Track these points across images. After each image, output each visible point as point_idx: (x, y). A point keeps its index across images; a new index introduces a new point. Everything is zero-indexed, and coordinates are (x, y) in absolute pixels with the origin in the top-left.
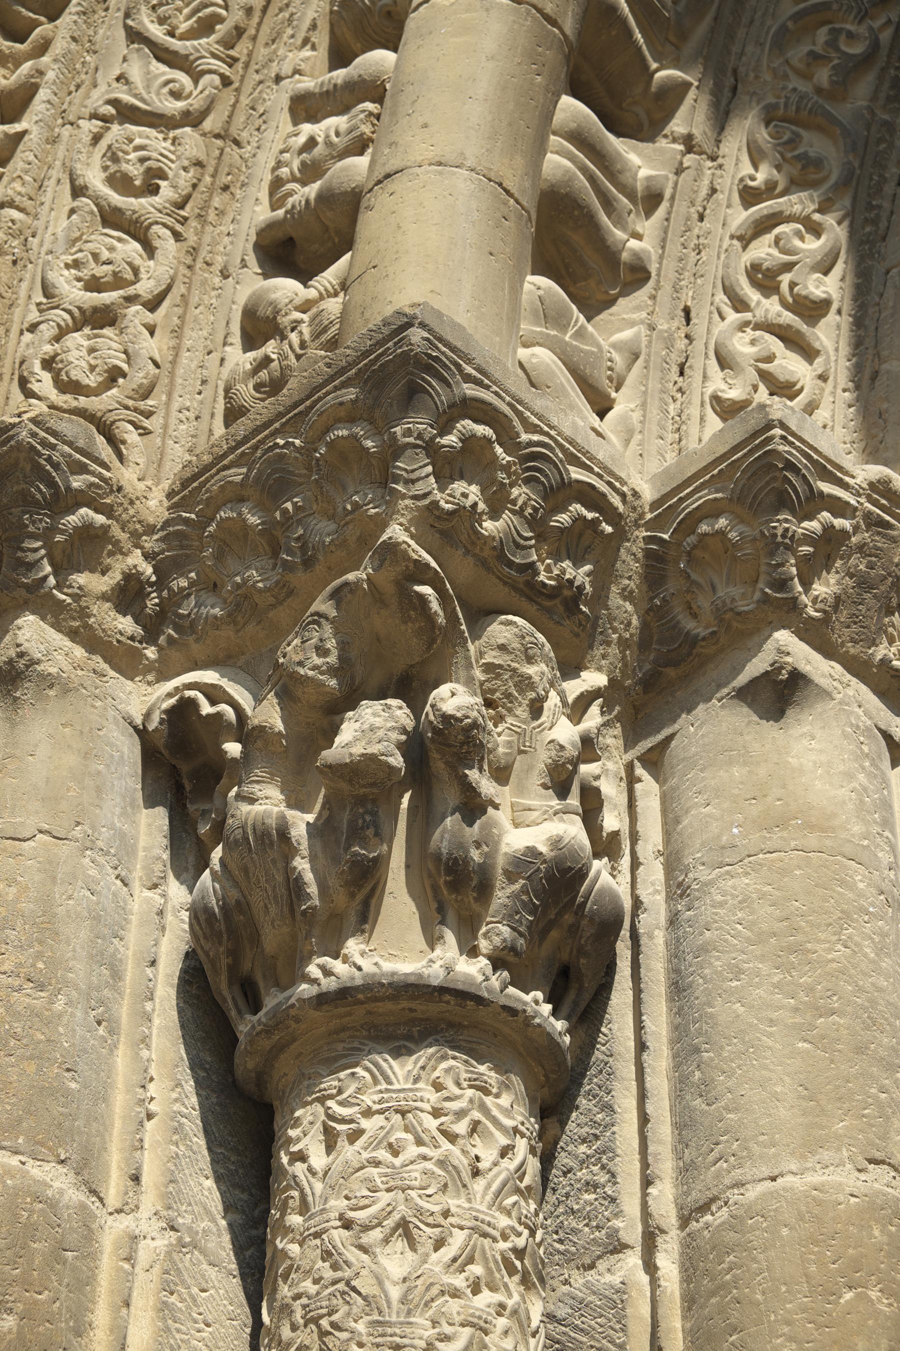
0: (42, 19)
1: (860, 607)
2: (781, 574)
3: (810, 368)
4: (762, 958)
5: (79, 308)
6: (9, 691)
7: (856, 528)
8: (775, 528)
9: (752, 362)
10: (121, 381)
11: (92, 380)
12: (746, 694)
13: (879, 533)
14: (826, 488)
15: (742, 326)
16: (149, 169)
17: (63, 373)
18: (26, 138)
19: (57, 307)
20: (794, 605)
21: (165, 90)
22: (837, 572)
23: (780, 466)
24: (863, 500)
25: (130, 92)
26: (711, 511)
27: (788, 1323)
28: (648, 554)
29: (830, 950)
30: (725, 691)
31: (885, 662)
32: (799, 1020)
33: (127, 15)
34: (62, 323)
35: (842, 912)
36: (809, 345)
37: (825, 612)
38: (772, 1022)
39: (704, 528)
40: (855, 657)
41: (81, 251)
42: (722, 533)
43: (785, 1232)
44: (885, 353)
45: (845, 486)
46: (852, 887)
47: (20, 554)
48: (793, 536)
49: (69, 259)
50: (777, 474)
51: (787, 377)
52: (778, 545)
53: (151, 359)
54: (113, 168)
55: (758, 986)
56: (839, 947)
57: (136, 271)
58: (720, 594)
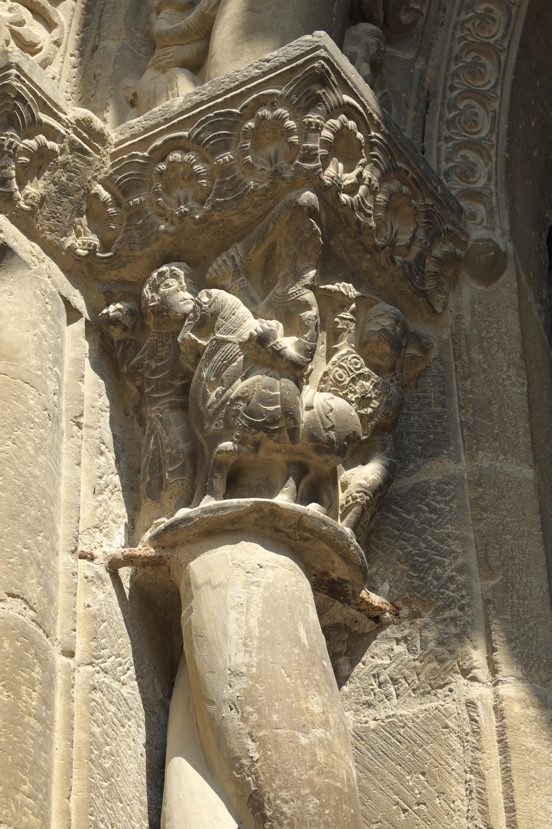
1: (59, 207)
2: (4, 174)
3: (49, 35)
7: (63, 151)
8: (3, 140)
13: (79, 157)
14: (45, 118)
20: (10, 197)
22: (45, 180)
23: (13, 96)
24: (70, 131)
31: (72, 249)
35: (15, 419)
36: (50, 19)
37: (32, 206)
40: (50, 242)
44: (104, 34)
45: (59, 119)
46: (24, 402)
48: (16, 148)
50: (10, 101)
51: (32, 39)
52: (4, 153)
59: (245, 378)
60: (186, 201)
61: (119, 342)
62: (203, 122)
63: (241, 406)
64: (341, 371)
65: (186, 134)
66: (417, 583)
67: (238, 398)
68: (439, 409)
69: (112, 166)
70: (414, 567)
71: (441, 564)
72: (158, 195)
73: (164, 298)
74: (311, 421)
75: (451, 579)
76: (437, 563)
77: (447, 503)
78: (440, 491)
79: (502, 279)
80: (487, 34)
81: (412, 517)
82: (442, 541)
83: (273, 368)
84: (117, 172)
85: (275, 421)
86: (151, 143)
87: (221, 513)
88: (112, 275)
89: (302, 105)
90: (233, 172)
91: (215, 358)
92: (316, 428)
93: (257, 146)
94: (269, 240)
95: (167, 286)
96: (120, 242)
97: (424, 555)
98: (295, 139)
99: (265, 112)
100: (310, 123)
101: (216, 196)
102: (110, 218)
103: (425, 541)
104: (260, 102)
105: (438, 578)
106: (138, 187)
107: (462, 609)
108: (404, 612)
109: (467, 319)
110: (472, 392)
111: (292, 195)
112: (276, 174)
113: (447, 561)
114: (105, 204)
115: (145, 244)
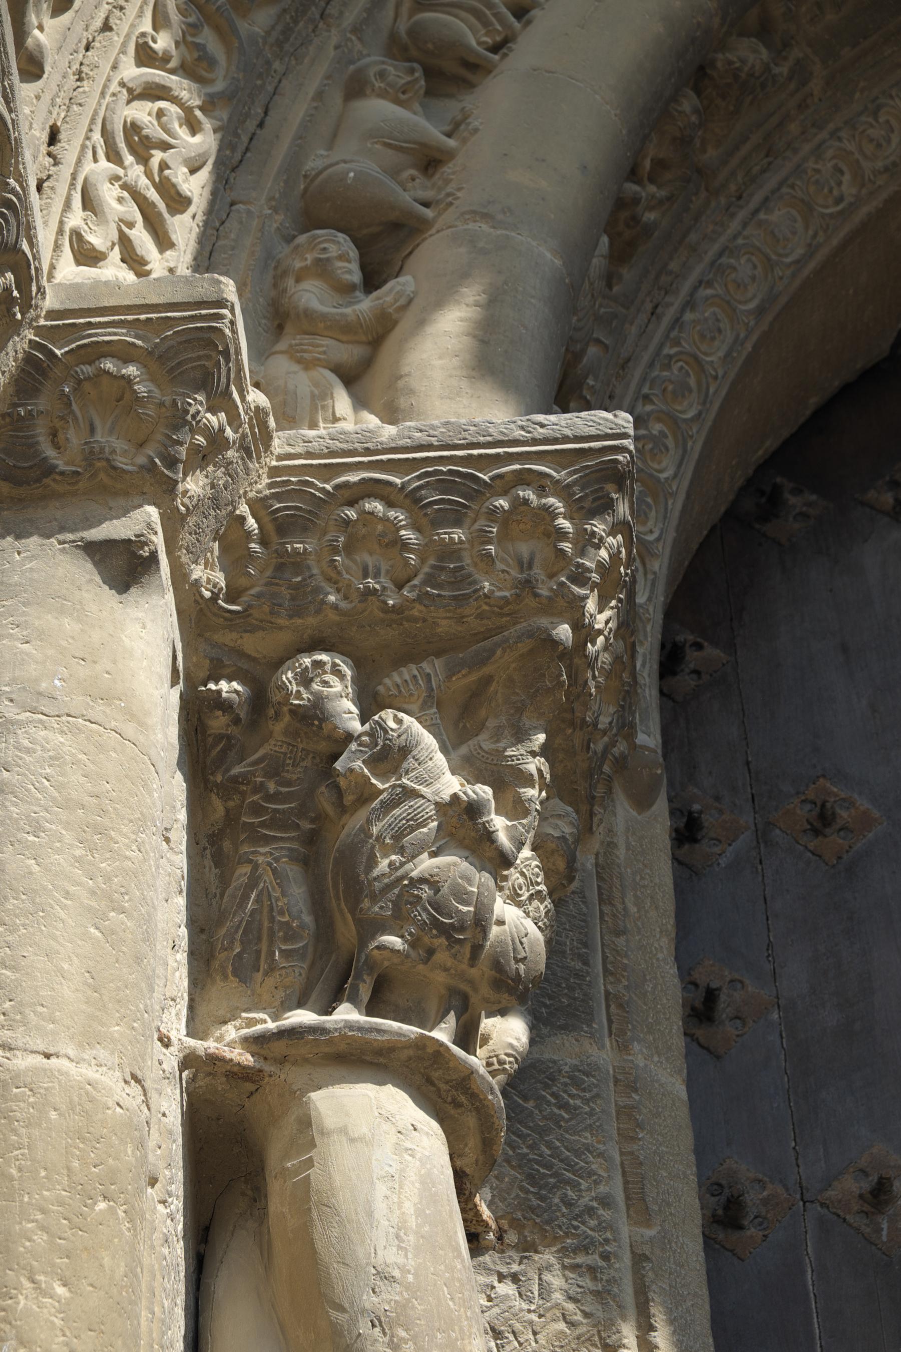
1: (204, 520)
2: (176, 452)
3: (160, 256)
4: (67, 825)
8: (190, 404)
9: (117, 219)
12: (93, 549)
13: (243, 459)
15: (114, 179)
22: (207, 477)
23: (220, 349)
26: (125, 353)
27: (43, 1211)
28: (29, 359)
29: (128, 847)
30: (70, 536)
32: (93, 904)
35: (142, 813)
36: (166, 233)
37: (188, 509)
38: (67, 895)
39: (109, 365)
40: (182, 565)
42: (128, 380)
43: (53, 1115)
48: (200, 421)
50: (214, 354)
51: (144, 253)
52: (187, 422)
55: (58, 851)
56: (134, 847)
58: (98, 437)
59: (433, 855)
60: (376, 576)
61: (220, 737)
62: (427, 474)
63: (426, 892)
64: (521, 880)
65: (398, 481)
66: (535, 1202)
67: (422, 880)
68: (578, 965)
69: (270, 486)
70: (531, 1178)
71: (575, 1186)
72: (335, 551)
73: (319, 702)
74: (500, 942)
75: (590, 1211)
76: (568, 1182)
77: (587, 1101)
78: (576, 1083)
79: (654, 808)
80: (656, 466)
81: (530, 1105)
82: (578, 1153)
83: (473, 852)
84: (277, 497)
85: (462, 929)
86: (339, 475)
87: (374, 1036)
88: (228, 638)
89: (587, 504)
90: (460, 559)
91: (396, 812)
92: (504, 954)
93: (504, 537)
94: (487, 670)
95: (326, 683)
96: (258, 596)
97: (549, 1166)
98: (567, 546)
99: (530, 494)
100: (593, 534)
101: (426, 582)
102: (250, 556)
103: (549, 1145)
104: (523, 479)
105: (569, 1204)
106: (305, 529)
107: (605, 1257)
108: (512, 1237)
109: (621, 852)
110: (626, 956)
111: (544, 622)
112: (527, 585)
113: (584, 1185)
114: (249, 534)
115: (297, 612)
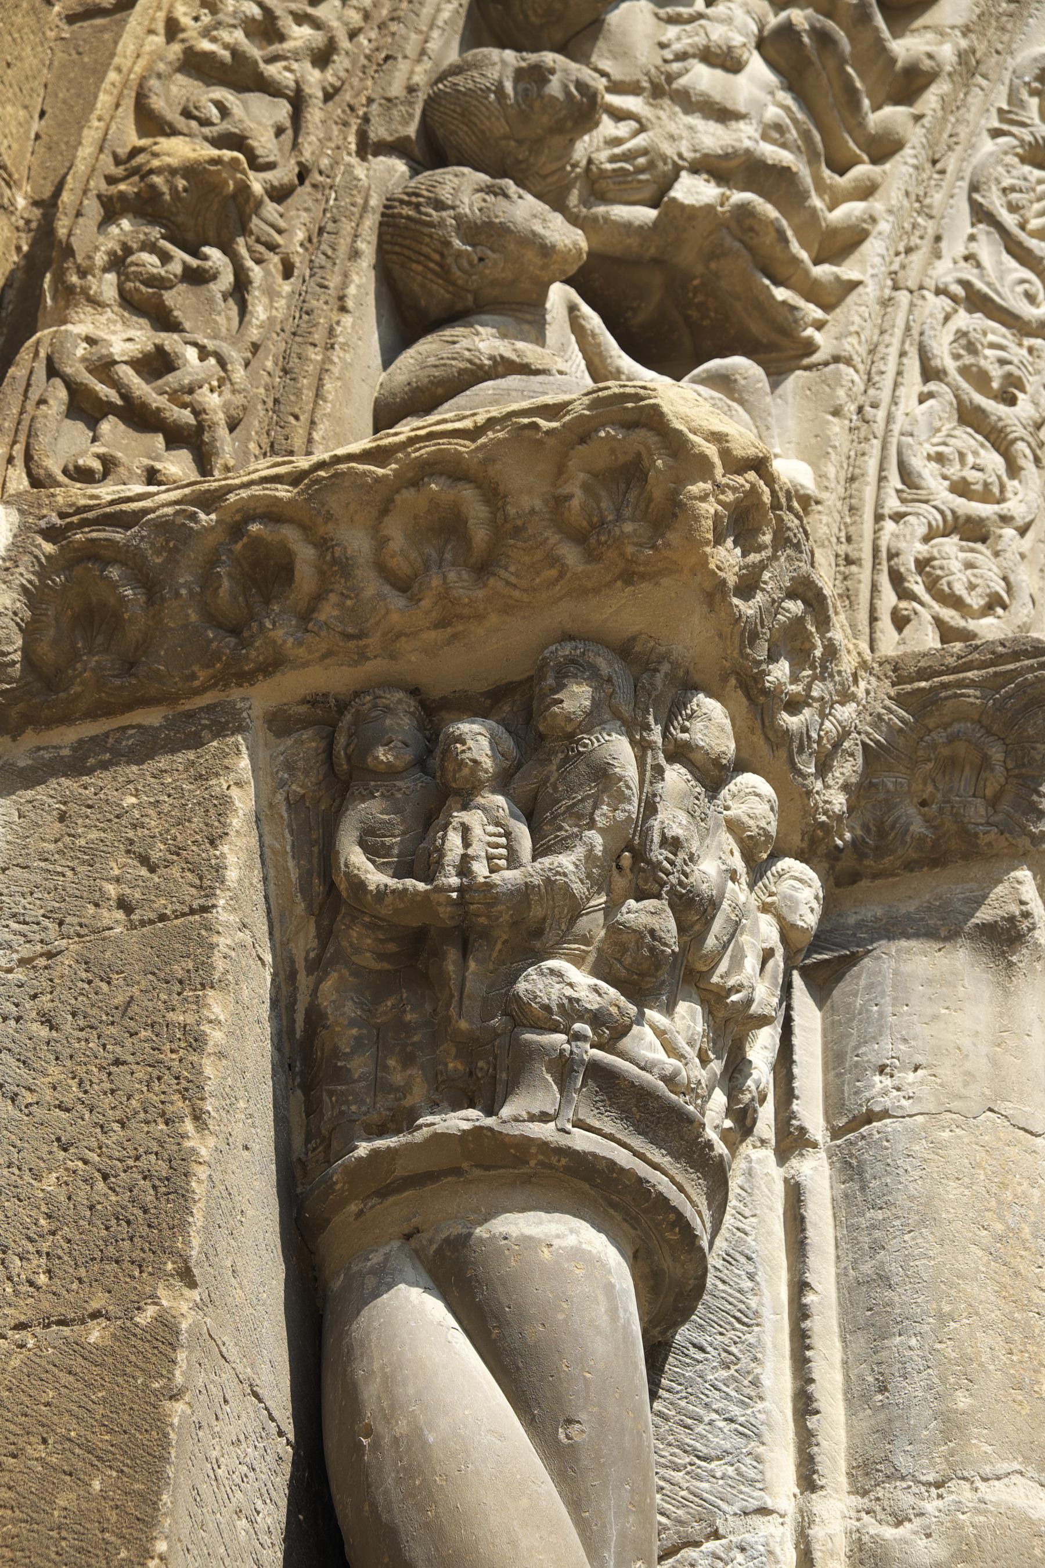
0: (865, 157)
5: (953, 512)
6: (1004, 952)
10: (999, 611)
11: (975, 601)
16: (1009, 375)
17: (944, 581)
18: (860, 289)
19: (926, 502)
21: (1020, 289)
25: (982, 277)
33: (974, 188)
34: (934, 523)
41: (945, 444)
47: (1035, 798)
49: (933, 450)
53: (1031, 596)
54: (968, 360)
57: (1002, 488)
